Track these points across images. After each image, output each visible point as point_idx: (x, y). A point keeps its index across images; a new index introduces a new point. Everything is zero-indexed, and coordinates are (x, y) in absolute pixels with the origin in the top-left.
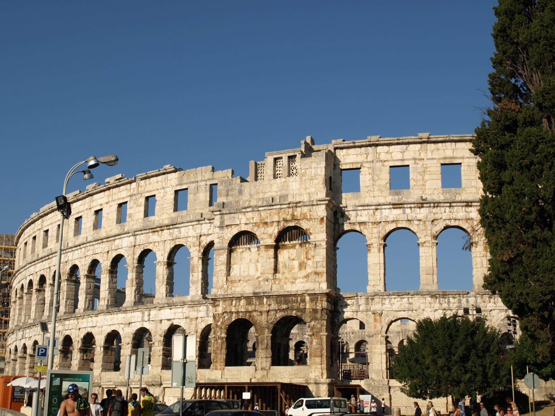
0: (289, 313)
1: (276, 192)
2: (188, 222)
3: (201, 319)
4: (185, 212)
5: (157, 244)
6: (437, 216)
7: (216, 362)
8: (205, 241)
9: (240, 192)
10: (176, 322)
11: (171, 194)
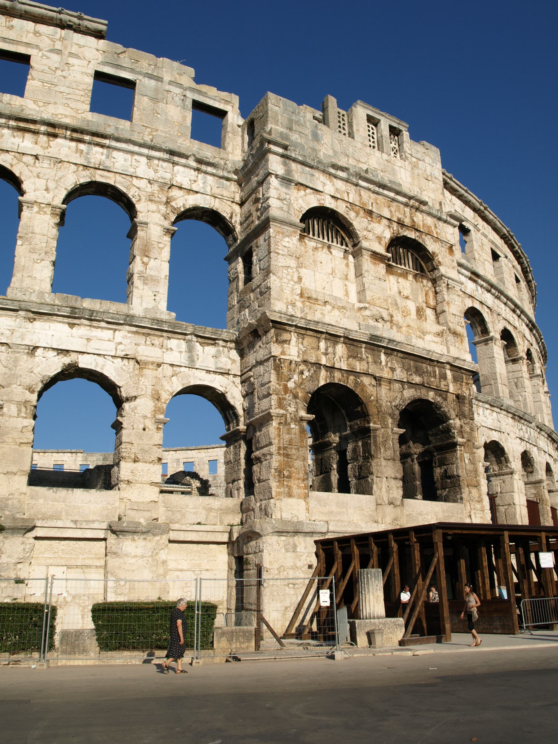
0: (422, 394)
2: (141, 145)
3: (170, 368)
4: (124, 124)
7: (289, 477)
10: (85, 362)
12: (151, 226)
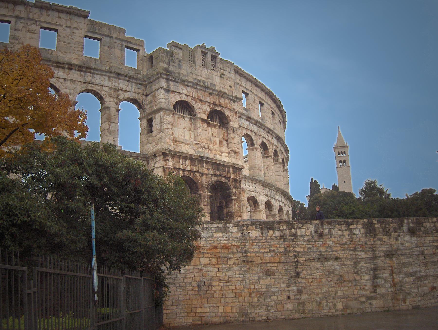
2: (106, 72)
12: (111, 108)
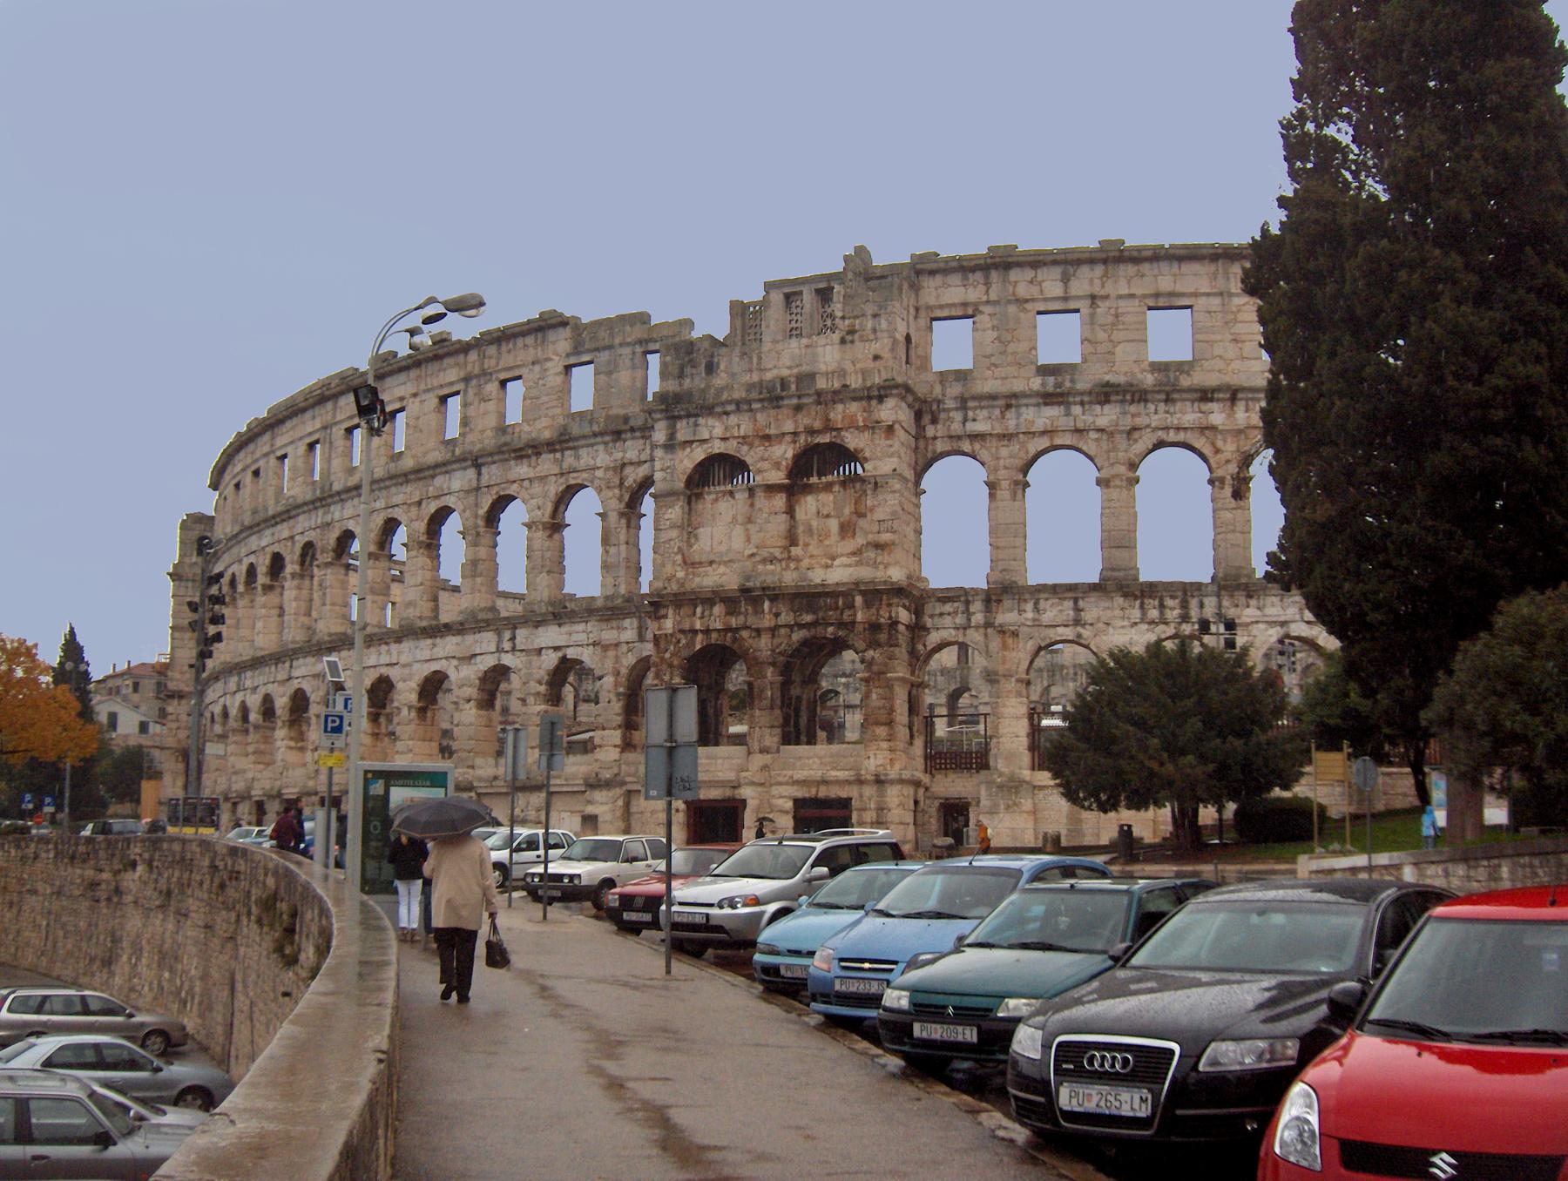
1: (790, 368)
5: (526, 483)
6: (1139, 421)
8: (633, 475)
9: (711, 369)
10: (571, 653)
11: (557, 374)
